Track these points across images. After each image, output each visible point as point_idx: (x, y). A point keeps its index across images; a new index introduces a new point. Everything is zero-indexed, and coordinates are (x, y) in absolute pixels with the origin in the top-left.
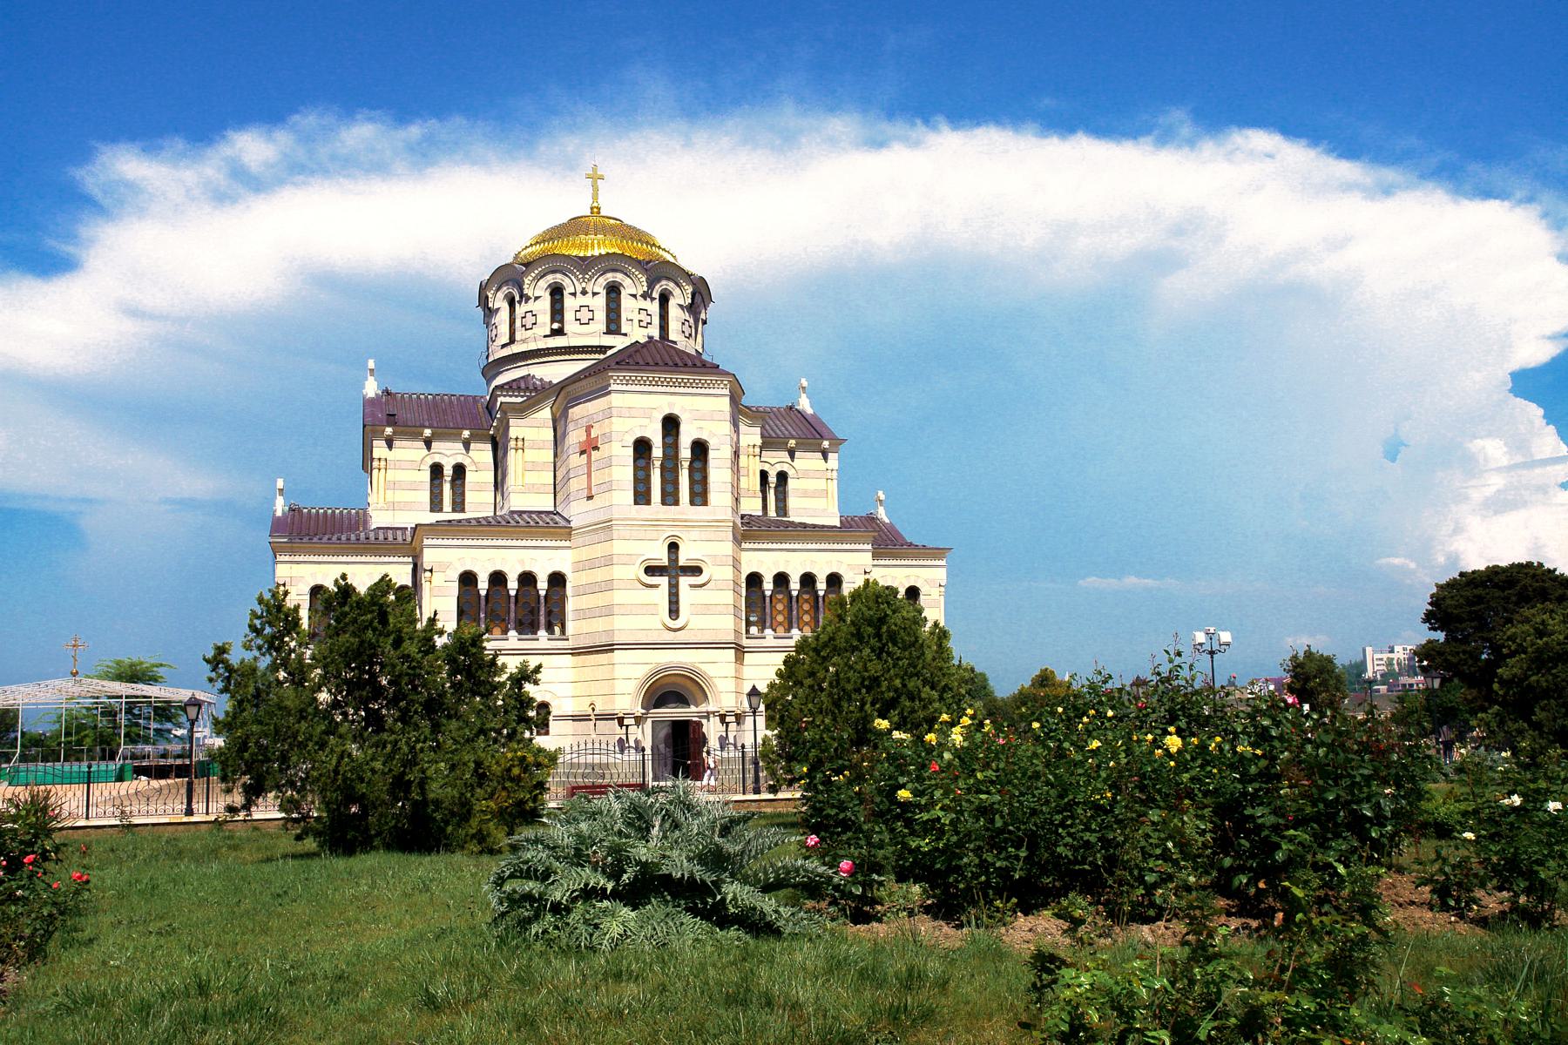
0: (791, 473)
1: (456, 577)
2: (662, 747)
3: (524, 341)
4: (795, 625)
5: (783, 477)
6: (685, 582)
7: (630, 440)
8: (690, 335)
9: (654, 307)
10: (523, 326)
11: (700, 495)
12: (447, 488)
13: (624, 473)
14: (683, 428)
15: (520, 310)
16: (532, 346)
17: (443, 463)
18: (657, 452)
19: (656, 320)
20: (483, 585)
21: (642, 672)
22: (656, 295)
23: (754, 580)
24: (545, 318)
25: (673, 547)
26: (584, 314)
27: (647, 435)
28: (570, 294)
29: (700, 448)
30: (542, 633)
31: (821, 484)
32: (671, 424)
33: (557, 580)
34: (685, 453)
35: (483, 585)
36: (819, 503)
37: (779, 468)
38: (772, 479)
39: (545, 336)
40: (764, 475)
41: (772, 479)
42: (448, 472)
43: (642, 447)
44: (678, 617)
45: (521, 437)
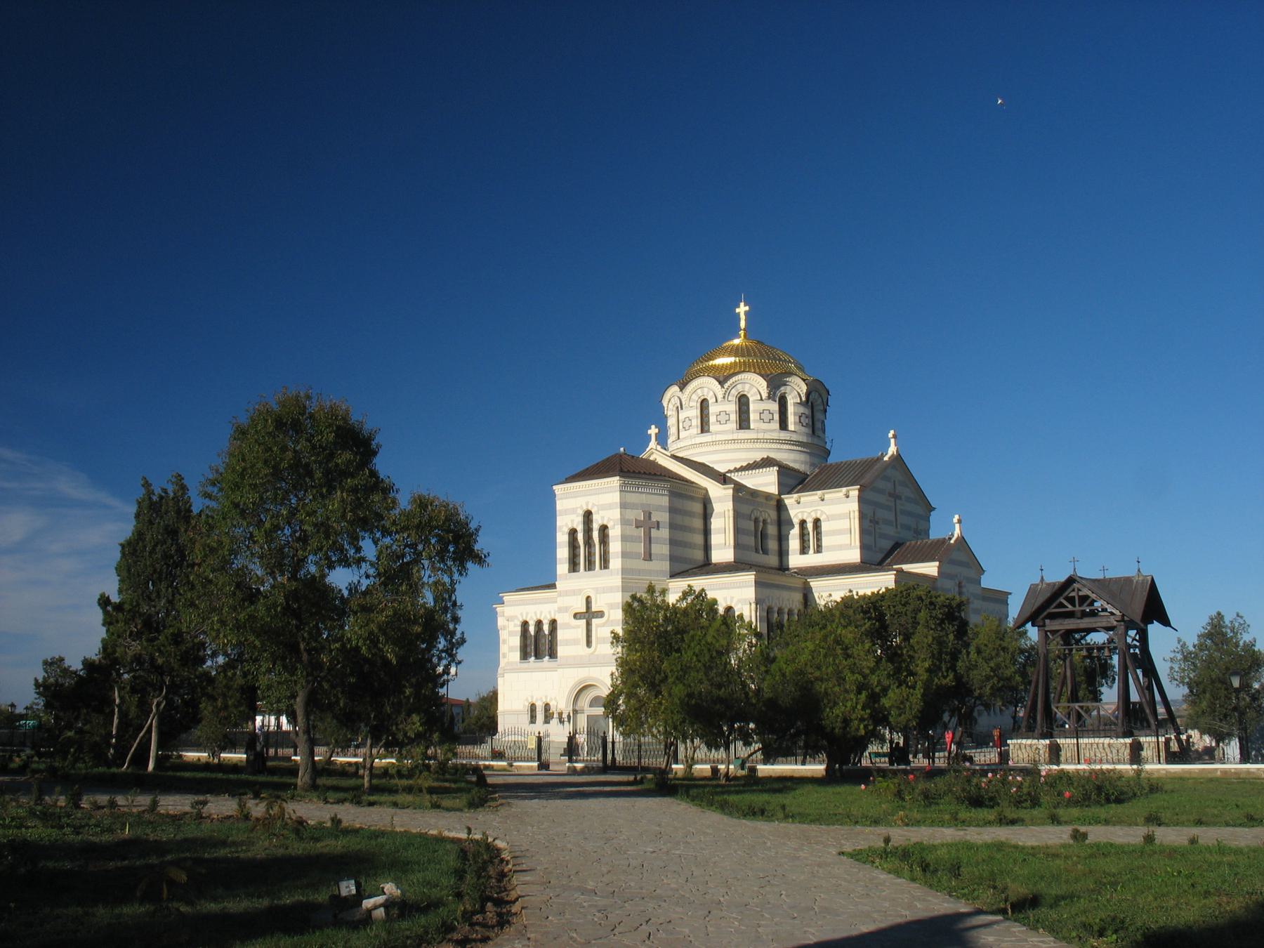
1: (519, 623)
5: (817, 522)
6: (595, 622)
7: (566, 530)
9: (732, 408)
11: (605, 564)
13: (563, 553)
19: (734, 417)
20: (532, 629)
21: (571, 683)
25: (588, 600)
26: (687, 424)
27: (575, 527)
29: (604, 529)
31: (844, 524)
32: (588, 516)
34: (595, 535)
35: (532, 629)
36: (845, 539)
38: (810, 526)
41: (810, 526)
43: (573, 533)
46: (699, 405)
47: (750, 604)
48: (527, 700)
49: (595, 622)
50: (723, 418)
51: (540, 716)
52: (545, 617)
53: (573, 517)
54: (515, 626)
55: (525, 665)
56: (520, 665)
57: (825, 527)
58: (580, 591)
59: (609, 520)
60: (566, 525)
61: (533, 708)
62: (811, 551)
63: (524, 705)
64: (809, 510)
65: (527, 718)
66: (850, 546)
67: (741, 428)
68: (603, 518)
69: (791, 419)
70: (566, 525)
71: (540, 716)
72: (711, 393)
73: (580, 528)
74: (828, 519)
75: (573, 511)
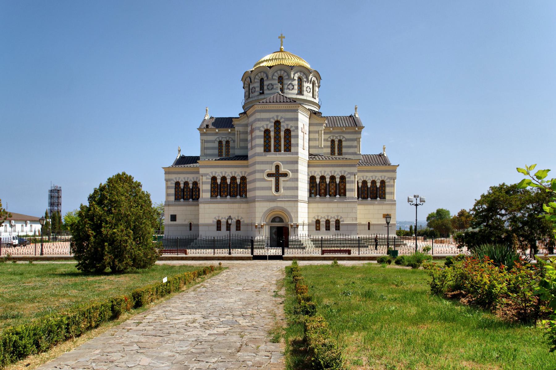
0: (344, 139)
2: (274, 236)
3: (252, 97)
4: (328, 193)
5: (340, 141)
6: (282, 179)
8: (310, 92)
9: (296, 83)
10: (251, 92)
12: (224, 148)
14: (282, 124)
15: (251, 87)
16: (254, 99)
17: (222, 140)
18: (272, 134)
19: (296, 87)
20: (219, 181)
21: (265, 209)
22: (296, 78)
23: (312, 179)
24: (258, 89)
25: (277, 167)
26: (270, 87)
27: (269, 128)
28: (266, 80)
29: (288, 132)
30: (238, 197)
32: (277, 124)
33: (243, 179)
34: (282, 134)
35: (219, 181)
37: (339, 138)
38: (336, 143)
39: (258, 95)
40: (333, 141)
41: (336, 143)
42: (224, 143)
43: (267, 132)
44: (279, 191)
45: (239, 130)
46: (277, 79)
47: (355, 175)
48: (215, 218)
49: (282, 179)
50: (291, 87)
51: (224, 227)
52: (228, 175)
53: (268, 123)
54: (207, 179)
55: (215, 200)
56: (210, 200)
57: (344, 144)
58: (272, 163)
59: (291, 127)
60: (263, 127)
61: (219, 223)
62: (336, 154)
63: (213, 221)
64: (337, 135)
65: (215, 228)
66: (355, 154)
67: (297, 94)
68: (287, 125)
69: (316, 93)
70: (263, 127)
71: (224, 227)
72: (286, 74)
73: (272, 129)
74: (347, 140)
75: (268, 120)
